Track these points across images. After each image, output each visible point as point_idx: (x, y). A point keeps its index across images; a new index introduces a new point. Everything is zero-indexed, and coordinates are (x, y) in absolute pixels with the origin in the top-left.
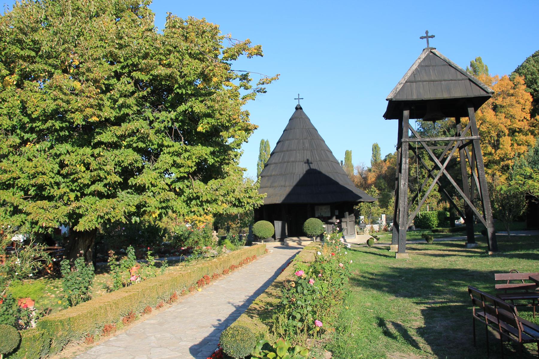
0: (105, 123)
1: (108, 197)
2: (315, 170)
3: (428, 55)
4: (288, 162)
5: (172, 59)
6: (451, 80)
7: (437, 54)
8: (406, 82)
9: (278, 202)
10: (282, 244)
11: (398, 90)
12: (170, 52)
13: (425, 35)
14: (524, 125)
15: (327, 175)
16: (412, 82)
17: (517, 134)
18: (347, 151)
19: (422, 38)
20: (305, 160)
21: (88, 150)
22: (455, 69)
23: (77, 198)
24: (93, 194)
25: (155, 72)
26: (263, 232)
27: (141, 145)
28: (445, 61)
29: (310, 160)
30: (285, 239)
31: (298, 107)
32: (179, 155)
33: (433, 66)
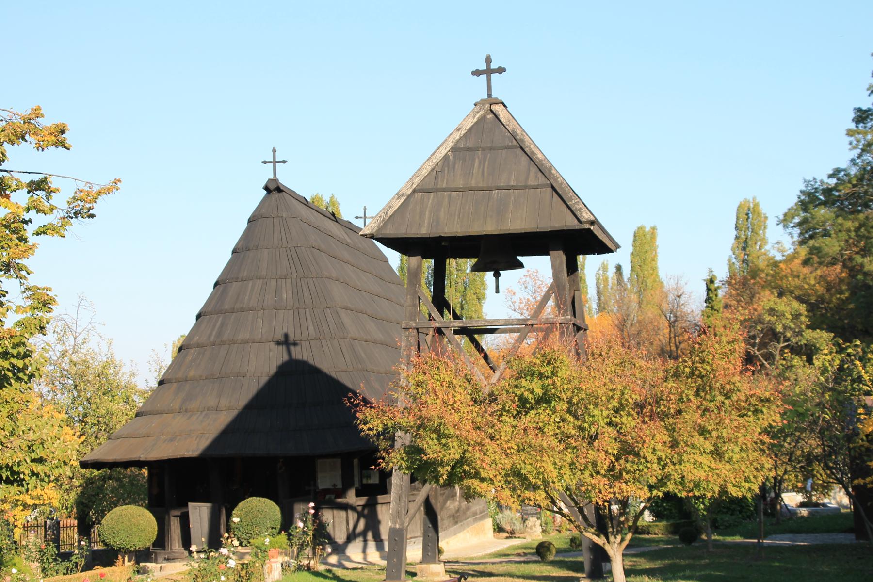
3: (482, 119)
4: (232, 343)
8: (415, 191)
11: (390, 212)
13: (483, 67)
15: (333, 375)
16: (428, 191)
18: (641, 228)
19: (477, 73)
22: (531, 158)
26: (123, 535)
28: (514, 136)
31: (272, 187)
33: (484, 149)
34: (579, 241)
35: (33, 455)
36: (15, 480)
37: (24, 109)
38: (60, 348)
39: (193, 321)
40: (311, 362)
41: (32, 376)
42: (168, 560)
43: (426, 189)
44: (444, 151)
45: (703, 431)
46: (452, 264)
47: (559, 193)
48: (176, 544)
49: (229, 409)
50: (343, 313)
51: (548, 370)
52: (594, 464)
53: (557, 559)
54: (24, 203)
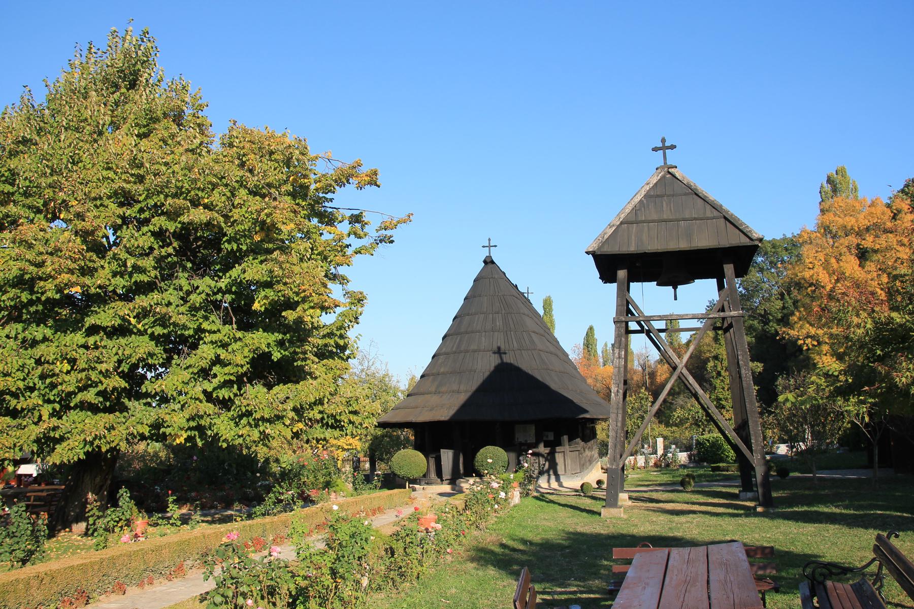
0: (102, 298)
1: (110, 410)
2: (511, 364)
3: (663, 177)
4: (467, 351)
5: (217, 198)
6: (695, 219)
7: (677, 175)
8: (622, 223)
9: (443, 419)
10: (453, 489)
11: (606, 237)
12: (215, 186)
13: (660, 145)
16: (632, 223)
19: (655, 149)
20: (495, 348)
21: (79, 338)
22: (705, 200)
23: (55, 414)
24: (84, 406)
25: (185, 219)
26: (405, 469)
27: (159, 330)
28: (688, 186)
29: (503, 347)
30: (458, 482)
31: (488, 260)
32: (225, 346)
35: (350, 409)
36: (338, 426)
37: (350, 162)
38: (360, 367)
40: (516, 364)
41: (349, 357)
42: (427, 484)
43: (632, 221)
47: (730, 221)
48: (433, 475)
49: (466, 391)
50: (533, 335)
53: (696, 489)
54: (346, 232)
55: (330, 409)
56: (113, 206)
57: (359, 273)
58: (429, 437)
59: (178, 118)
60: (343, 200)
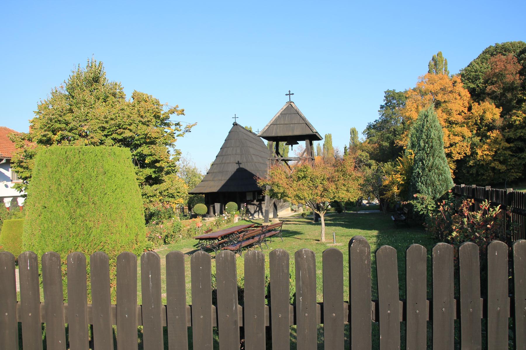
4: (225, 163)
13: (288, 93)
14: (460, 119)
17: (454, 126)
19: (287, 95)
22: (300, 116)
25: (124, 135)
28: (296, 111)
34: (313, 137)
37: (174, 106)
39: (215, 158)
43: (274, 124)
44: (278, 114)
45: (344, 185)
46: (281, 143)
47: (308, 125)
48: (212, 213)
51: (305, 170)
52: (317, 193)
55: (170, 191)
56: (100, 131)
57: (180, 143)
58: (211, 199)
59: (114, 95)
60: (173, 118)
